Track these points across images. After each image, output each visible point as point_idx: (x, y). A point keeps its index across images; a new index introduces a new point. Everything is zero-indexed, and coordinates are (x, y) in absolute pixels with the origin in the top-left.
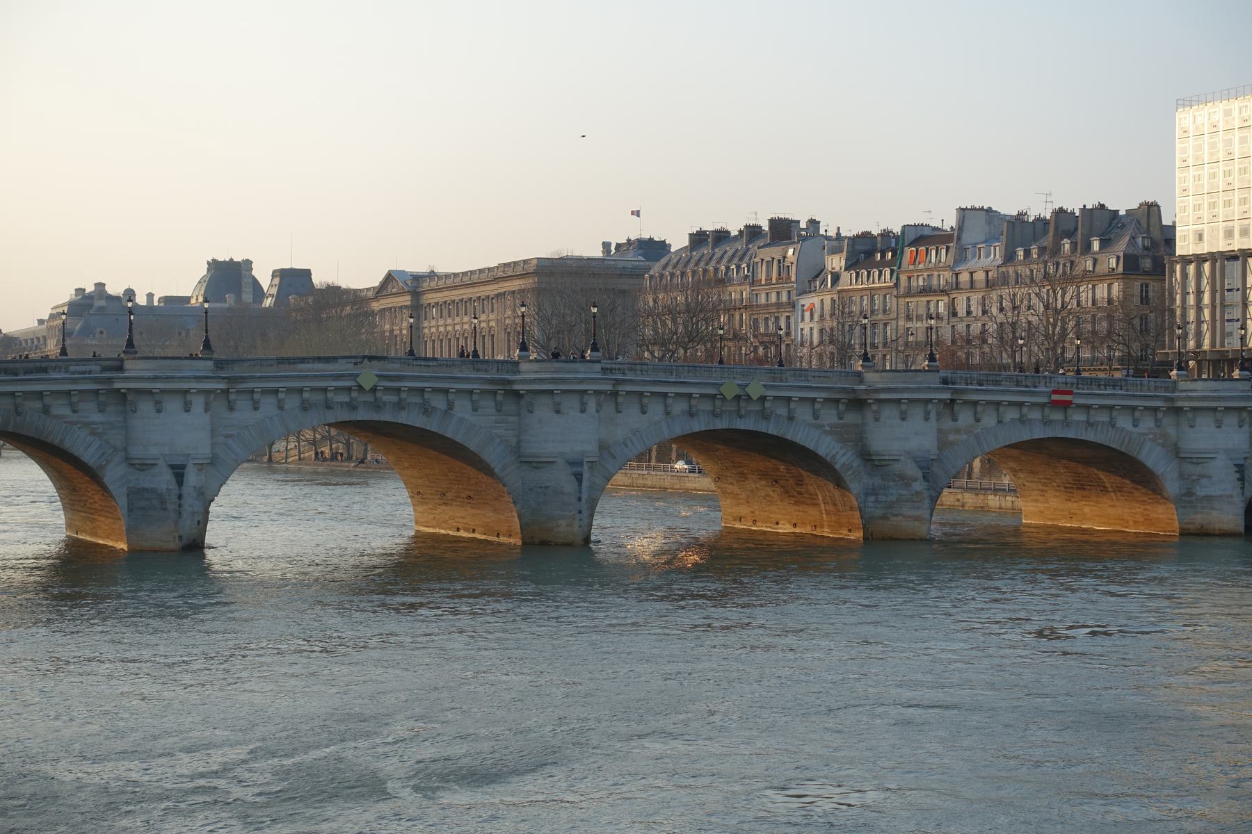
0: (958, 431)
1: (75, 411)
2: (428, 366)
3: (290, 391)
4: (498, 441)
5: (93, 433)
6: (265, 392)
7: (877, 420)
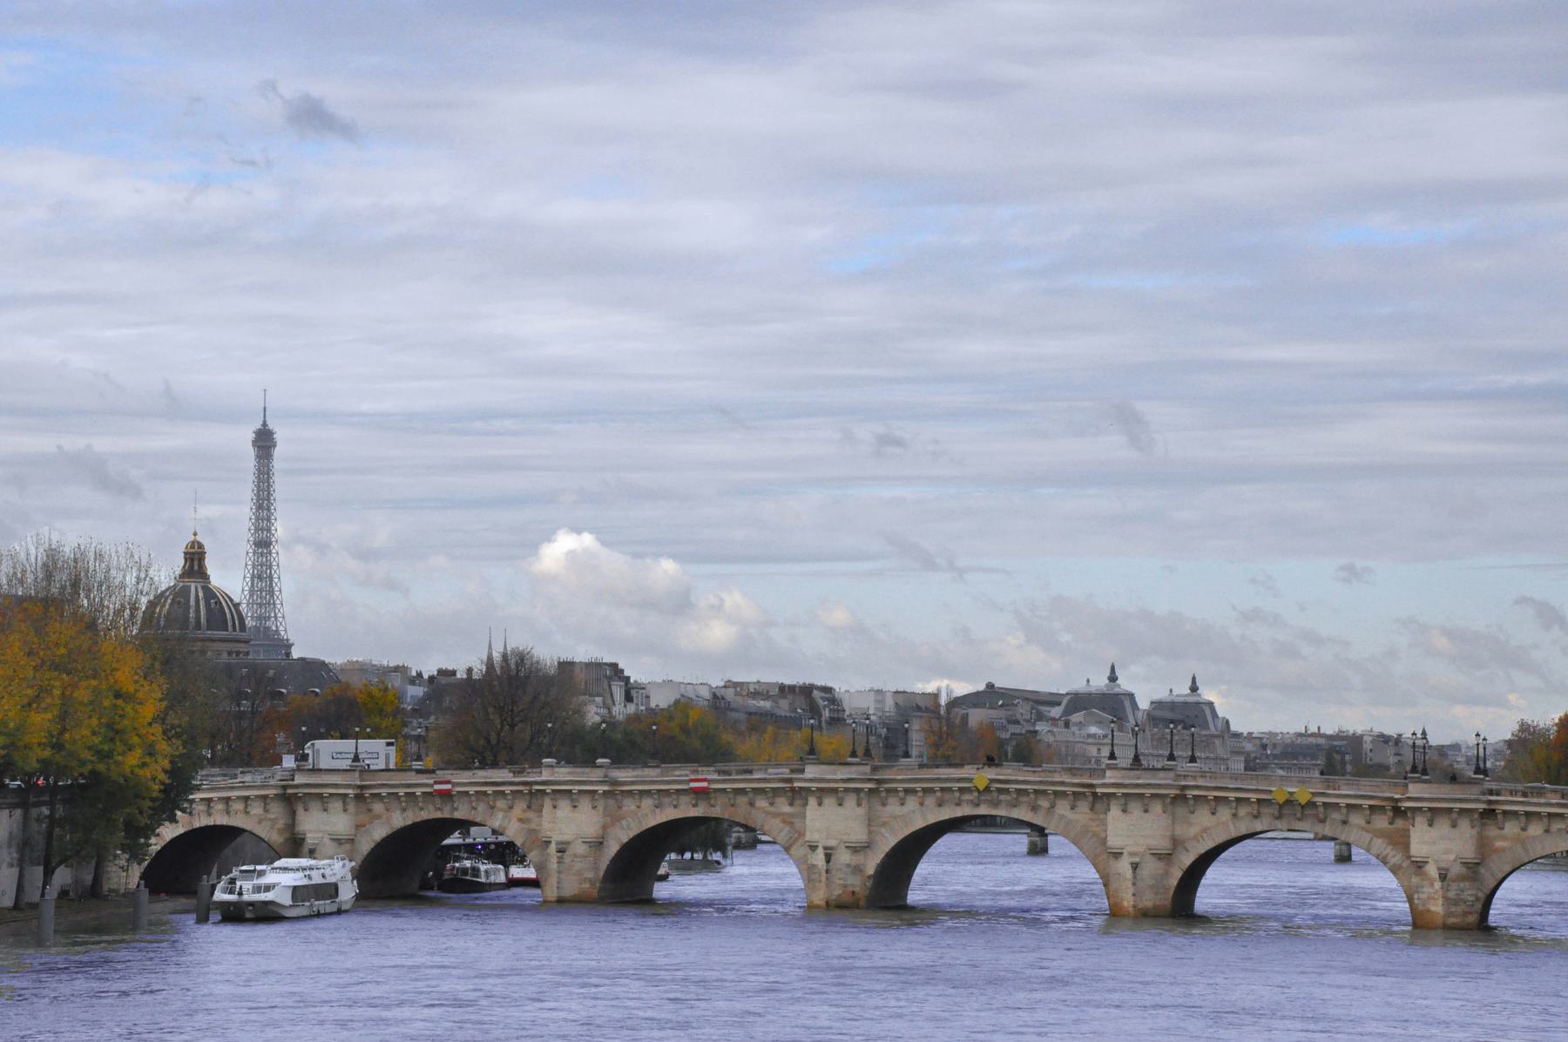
0: (1504, 838)
1: (772, 804)
2: (1035, 772)
3: (925, 790)
4: (1091, 834)
5: (784, 822)
6: (907, 791)
7: (1413, 826)
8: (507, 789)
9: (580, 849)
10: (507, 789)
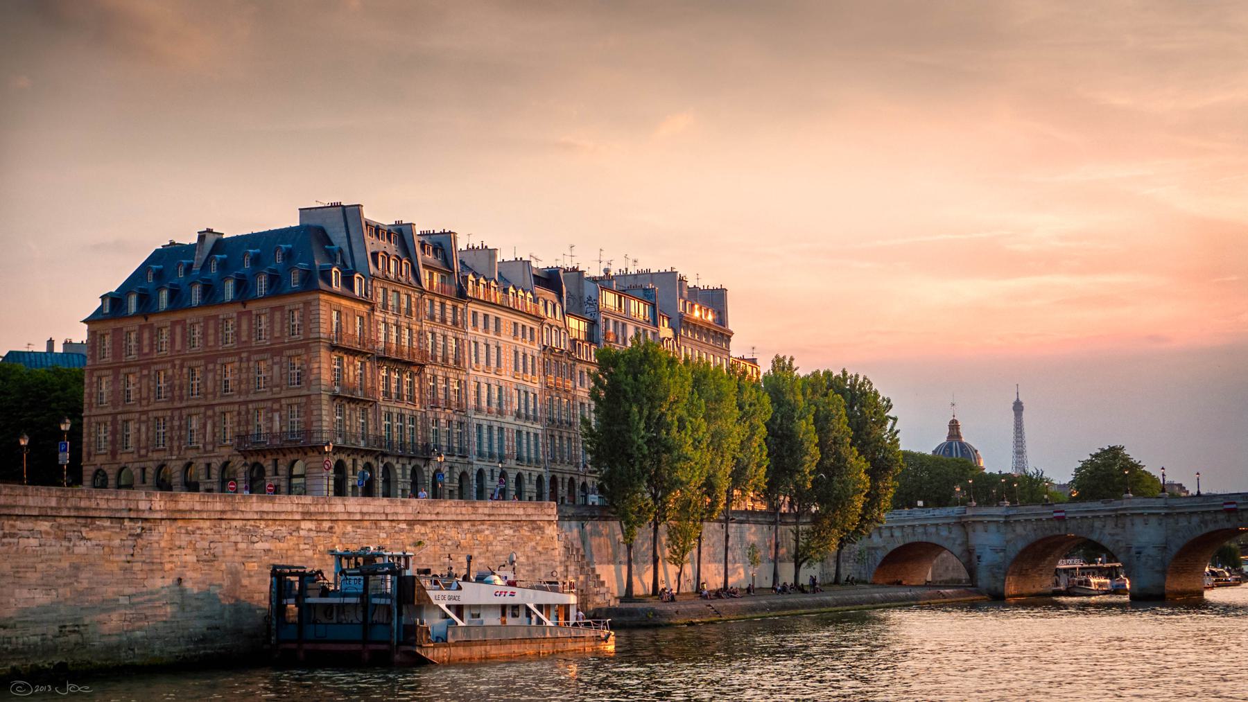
8: (1101, 514)
9: (1151, 551)
10: (1101, 514)
